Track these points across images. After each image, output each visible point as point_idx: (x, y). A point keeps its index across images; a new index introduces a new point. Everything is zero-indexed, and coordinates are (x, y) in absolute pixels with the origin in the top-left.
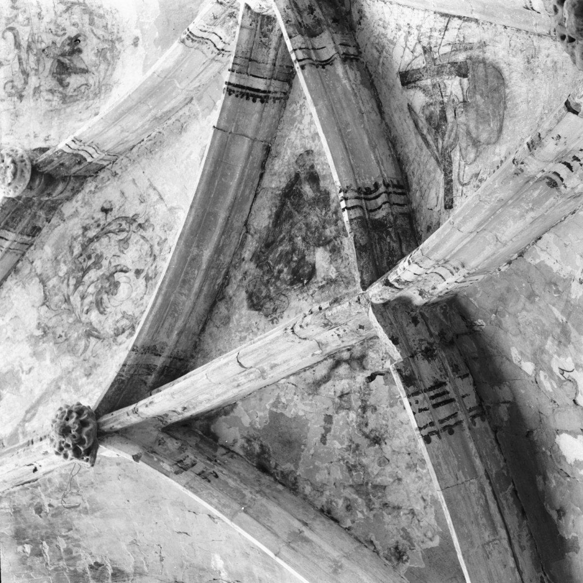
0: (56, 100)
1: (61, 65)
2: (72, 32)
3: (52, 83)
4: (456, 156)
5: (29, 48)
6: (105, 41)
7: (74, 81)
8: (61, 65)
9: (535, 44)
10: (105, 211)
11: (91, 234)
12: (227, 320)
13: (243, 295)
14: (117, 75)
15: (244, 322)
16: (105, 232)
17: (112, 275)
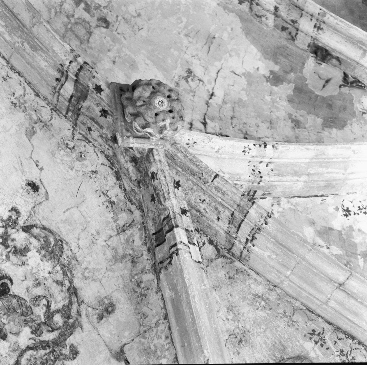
9: (227, 337)
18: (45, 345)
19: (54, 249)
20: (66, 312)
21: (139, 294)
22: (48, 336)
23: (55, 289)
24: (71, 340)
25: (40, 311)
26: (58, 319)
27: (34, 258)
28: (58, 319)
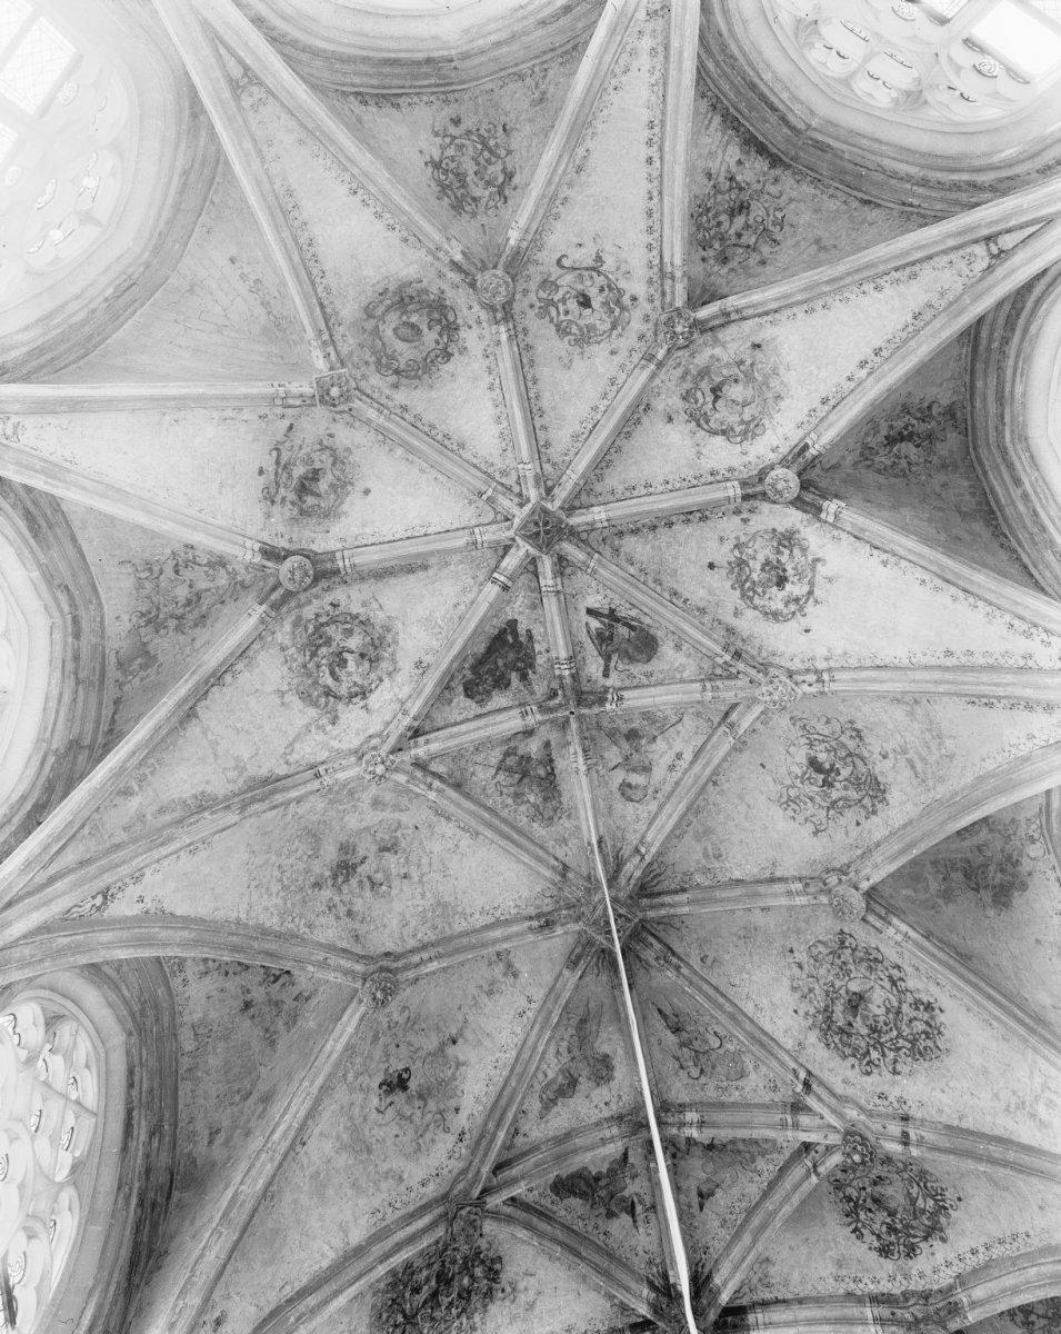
0: (296, 511)
1: (303, 485)
2: (317, 465)
3: (292, 496)
4: (615, 657)
5: (285, 467)
6: (338, 480)
7: (310, 500)
8: (303, 485)
10: (334, 605)
11: (323, 620)
12: (450, 702)
13: (461, 688)
14: (345, 507)
15: (462, 705)
16: (333, 621)
17: (341, 653)
18: (746, 581)
19: (775, 616)
20: (751, 599)
21: (730, 631)
22: (748, 585)
23: (762, 603)
24: (738, 591)
25: (760, 590)
26: (751, 594)
27: (780, 606)
28: (751, 594)
